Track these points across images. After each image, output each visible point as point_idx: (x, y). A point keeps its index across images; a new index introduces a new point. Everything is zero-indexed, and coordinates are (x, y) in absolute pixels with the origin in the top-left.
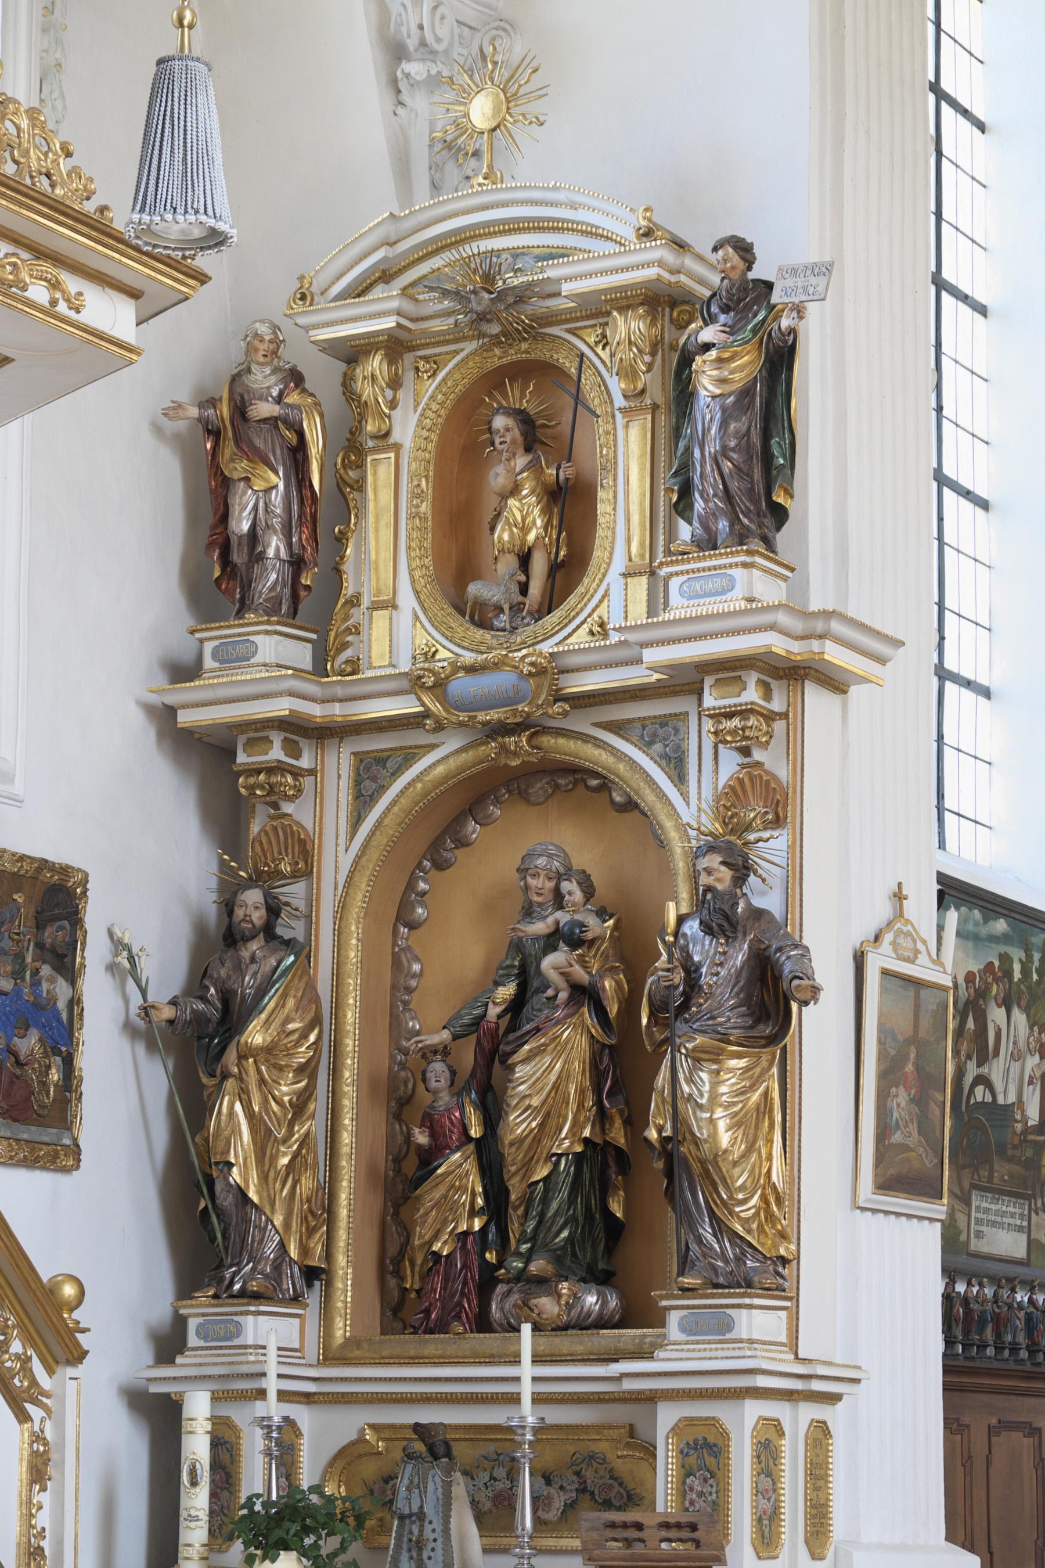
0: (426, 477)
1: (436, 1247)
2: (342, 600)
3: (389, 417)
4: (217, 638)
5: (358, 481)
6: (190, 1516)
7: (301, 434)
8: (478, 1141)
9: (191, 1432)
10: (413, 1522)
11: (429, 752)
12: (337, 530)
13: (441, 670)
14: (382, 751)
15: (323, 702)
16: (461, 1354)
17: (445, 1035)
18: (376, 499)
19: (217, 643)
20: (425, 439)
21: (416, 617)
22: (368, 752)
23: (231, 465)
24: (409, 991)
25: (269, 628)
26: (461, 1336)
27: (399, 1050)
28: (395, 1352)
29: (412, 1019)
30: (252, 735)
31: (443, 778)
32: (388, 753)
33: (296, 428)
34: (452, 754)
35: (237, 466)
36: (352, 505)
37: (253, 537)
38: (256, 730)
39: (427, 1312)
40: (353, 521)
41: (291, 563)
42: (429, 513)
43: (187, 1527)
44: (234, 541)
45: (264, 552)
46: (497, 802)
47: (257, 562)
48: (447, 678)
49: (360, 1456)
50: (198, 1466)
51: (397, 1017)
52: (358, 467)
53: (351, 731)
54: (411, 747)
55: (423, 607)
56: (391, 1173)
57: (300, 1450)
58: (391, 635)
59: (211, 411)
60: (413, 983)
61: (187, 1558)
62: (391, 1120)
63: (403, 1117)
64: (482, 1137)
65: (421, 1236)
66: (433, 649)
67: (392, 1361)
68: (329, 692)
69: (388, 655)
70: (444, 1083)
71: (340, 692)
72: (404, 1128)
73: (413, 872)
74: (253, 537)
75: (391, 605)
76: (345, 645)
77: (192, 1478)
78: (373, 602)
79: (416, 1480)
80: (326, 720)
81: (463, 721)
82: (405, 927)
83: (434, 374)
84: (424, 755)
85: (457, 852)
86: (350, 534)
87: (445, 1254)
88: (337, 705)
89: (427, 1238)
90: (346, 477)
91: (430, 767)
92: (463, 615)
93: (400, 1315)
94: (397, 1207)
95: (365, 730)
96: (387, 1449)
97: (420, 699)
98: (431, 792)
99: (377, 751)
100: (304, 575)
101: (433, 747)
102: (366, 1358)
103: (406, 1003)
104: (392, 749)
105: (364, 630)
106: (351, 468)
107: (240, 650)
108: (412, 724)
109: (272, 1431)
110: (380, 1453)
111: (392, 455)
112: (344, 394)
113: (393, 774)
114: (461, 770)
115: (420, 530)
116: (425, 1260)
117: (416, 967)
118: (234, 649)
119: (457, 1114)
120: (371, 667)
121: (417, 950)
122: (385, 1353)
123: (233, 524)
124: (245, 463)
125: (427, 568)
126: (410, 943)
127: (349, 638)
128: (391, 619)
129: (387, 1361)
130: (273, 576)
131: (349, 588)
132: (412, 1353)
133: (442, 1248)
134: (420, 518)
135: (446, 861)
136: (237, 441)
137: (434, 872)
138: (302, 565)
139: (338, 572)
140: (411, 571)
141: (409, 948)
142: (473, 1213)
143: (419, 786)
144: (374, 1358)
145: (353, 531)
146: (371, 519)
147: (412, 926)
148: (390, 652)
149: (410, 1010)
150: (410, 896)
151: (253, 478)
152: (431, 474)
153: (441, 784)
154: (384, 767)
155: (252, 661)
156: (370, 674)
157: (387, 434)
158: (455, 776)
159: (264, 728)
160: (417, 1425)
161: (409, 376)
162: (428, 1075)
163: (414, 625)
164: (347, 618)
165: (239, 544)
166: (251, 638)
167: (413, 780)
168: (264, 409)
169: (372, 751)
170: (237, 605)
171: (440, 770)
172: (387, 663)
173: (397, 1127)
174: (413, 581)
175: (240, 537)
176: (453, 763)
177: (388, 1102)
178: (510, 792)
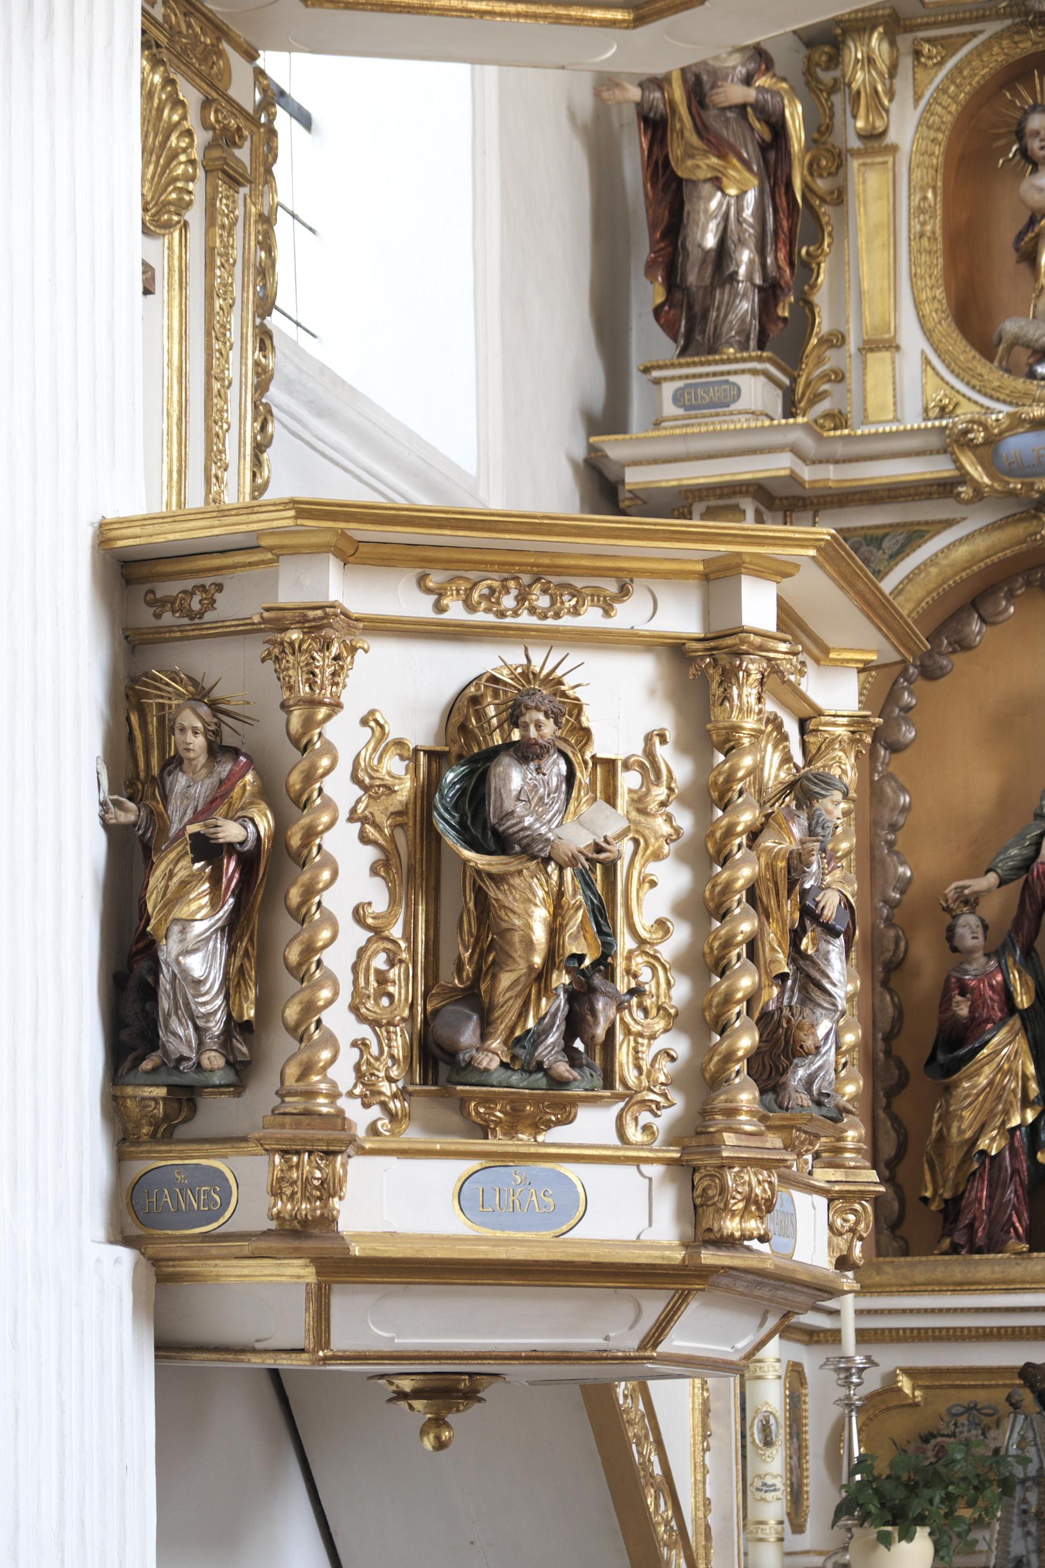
0: (934, 189)
1: (983, 1144)
2: (814, 341)
3: (887, 111)
4: (680, 378)
5: (832, 193)
6: (765, 1484)
7: (778, 129)
8: (1024, 1015)
9: (760, 1378)
10: (1027, 1489)
11: (945, 529)
12: (804, 251)
13: (994, 424)
14: (877, 527)
15: (814, 463)
16: (1029, 1279)
17: (992, 878)
18: (866, 214)
19: (680, 384)
20: (933, 140)
21: (927, 362)
22: (855, 529)
23: (689, 163)
24: (894, 828)
25: (759, 366)
26: (1025, 1256)
27: (886, 902)
28: (933, 1277)
29: (903, 863)
30: (713, 502)
31: (968, 561)
32: (884, 531)
33: (773, 120)
34: (980, 531)
35: (700, 163)
36: (825, 219)
37: (723, 253)
38: (721, 496)
39: (971, 1227)
40: (826, 242)
41: (761, 289)
42: (939, 232)
43: (763, 1499)
44: (695, 255)
45: (736, 273)
46: (1010, 596)
47: (722, 286)
48: (1001, 433)
49: (888, 1409)
50: (772, 1421)
51: (882, 862)
52: (830, 174)
53: (832, 502)
54: (919, 523)
55: (936, 350)
56: (881, 1055)
57: (805, 1403)
58: (894, 383)
59: (657, 95)
60: (901, 820)
61: (761, 1540)
62: (879, 989)
63: (891, 985)
64: (1031, 1007)
65: (961, 1132)
66: (954, 401)
67: (930, 1288)
68: (826, 450)
69: (892, 408)
70: (980, 942)
71: (840, 450)
72: (896, 999)
73: (896, 682)
74: (723, 253)
75: (892, 346)
76: (818, 397)
77: (766, 1437)
78: (865, 342)
79: (1030, 1435)
80: (820, 485)
81: (1015, 489)
82: (886, 749)
83: (941, 64)
84: (938, 533)
85: (954, 657)
86: (821, 258)
87: (993, 1153)
88: (831, 467)
89: (968, 1134)
90: (814, 187)
91: (948, 547)
92: (992, 361)
93: (898, 1232)
94: (890, 1094)
95: (853, 501)
96: (925, 1399)
97: (956, 461)
98: (949, 579)
99: (869, 528)
100: (781, 305)
101: (948, 524)
102: (891, 1285)
103: (891, 844)
104: (891, 526)
105: (853, 378)
106: (821, 176)
107: (715, 394)
108: (922, 494)
109: (851, 1375)
110: (916, 1405)
111: (890, 160)
112: (807, 84)
113: (892, 557)
114: (990, 553)
115: (930, 253)
116: (967, 1158)
117: (905, 799)
118: (707, 393)
119: (999, 978)
120: (865, 421)
121: (901, 779)
122: (920, 1278)
123: (693, 235)
124: (714, 160)
125: (939, 301)
126: (891, 769)
127: (826, 387)
128: (893, 362)
129: (923, 1288)
130: (745, 305)
131: (823, 325)
132: (959, 1276)
133: (990, 1145)
134: (929, 239)
135: (942, 668)
136: (702, 129)
137: (921, 684)
138: (779, 292)
139: (810, 306)
140: (917, 304)
141: (890, 776)
142: (1026, 1103)
143: (934, 570)
144: (902, 1285)
145: (827, 254)
146: (862, 240)
147: (895, 748)
148: (895, 404)
149: (897, 853)
150: (893, 711)
151: (725, 181)
152: (939, 184)
153: (964, 570)
154: (879, 547)
155: (733, 407)
156: (866, 430)
157: (884, 133)
158: (982, 560)
159: (734, 493)
160: (1028, 1365)
161: (906, 62)
162: (960, 931)
163: (924, 371)
164: (820, 362)
165: (704, 262)
166: (732, 379)
167: (924, 563)
168: (736, 93)
169: (863, 528)
170: (682, 342)
171: (962, 552)
172: (891, 417)
173: (888, 998)
174: (921, 319)
175: (707, 252)
176: (981, 544)
177: (873, 967)
178: (1028, 584)
